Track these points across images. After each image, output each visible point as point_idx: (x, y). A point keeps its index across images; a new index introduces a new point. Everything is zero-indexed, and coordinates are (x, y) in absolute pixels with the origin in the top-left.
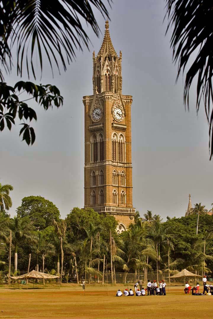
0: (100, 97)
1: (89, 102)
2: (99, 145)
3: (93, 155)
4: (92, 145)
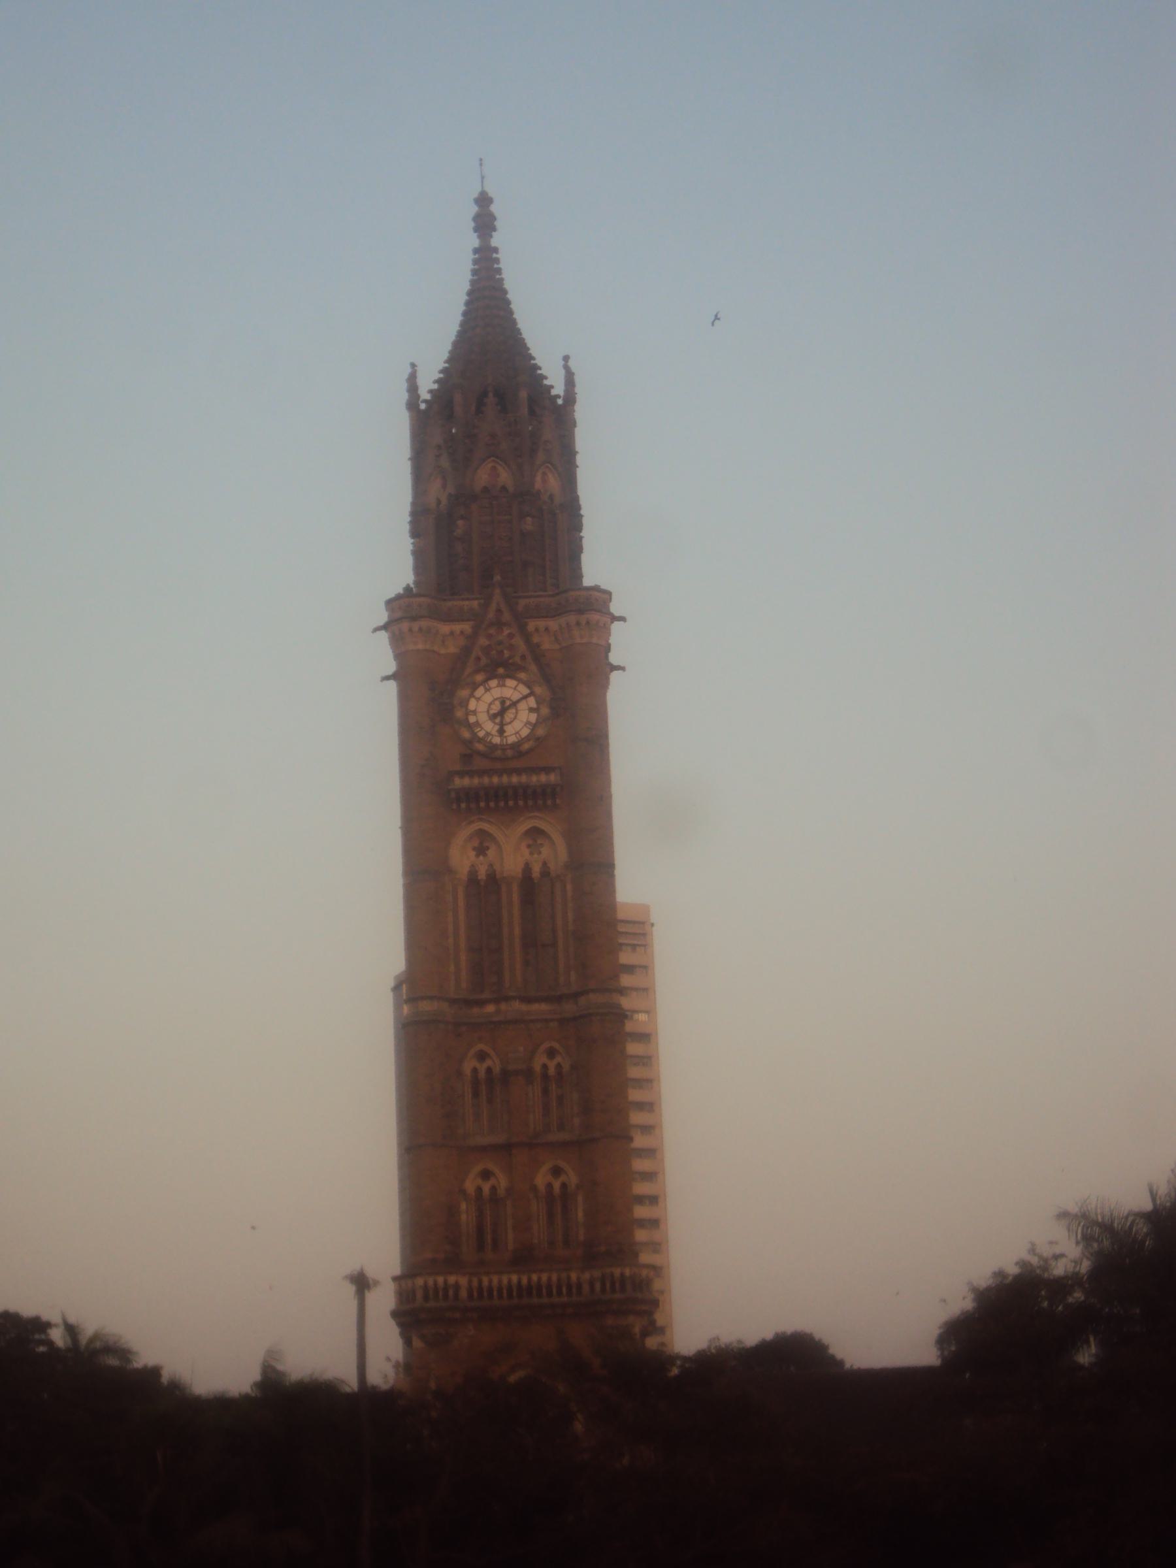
2: (515, 887)
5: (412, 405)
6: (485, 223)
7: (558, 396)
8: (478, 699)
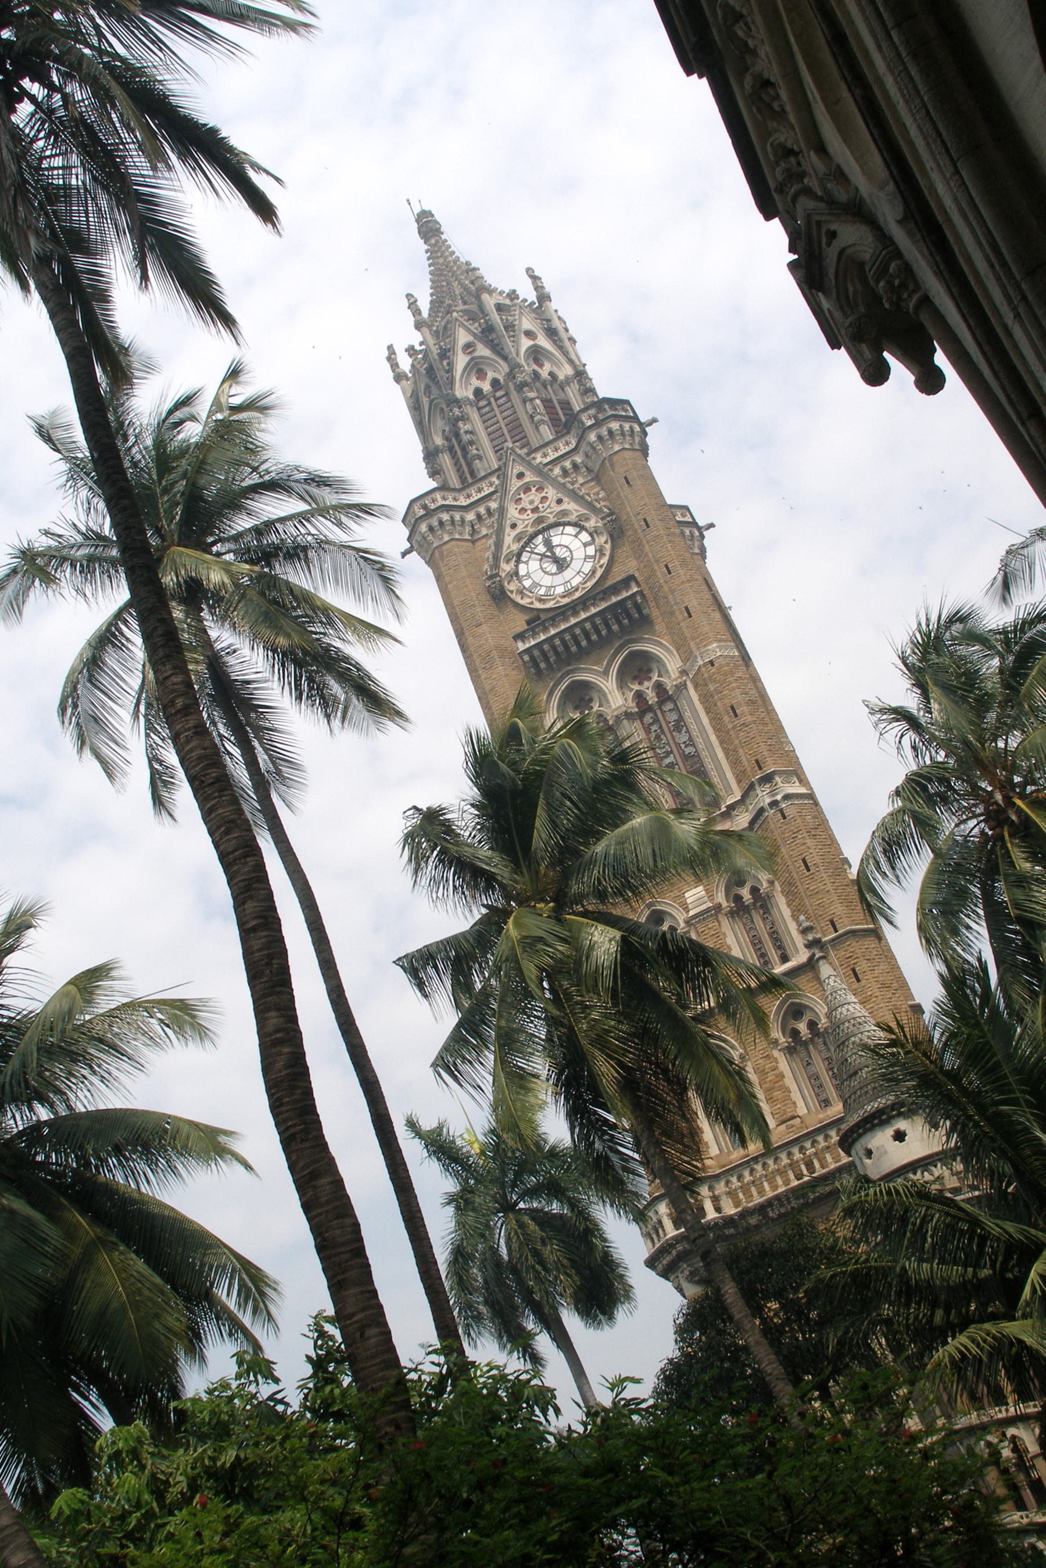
0: (549, 459)
5: (399, 377)
6: (428, 227)
7: (533, 303)
8: (527, 563)
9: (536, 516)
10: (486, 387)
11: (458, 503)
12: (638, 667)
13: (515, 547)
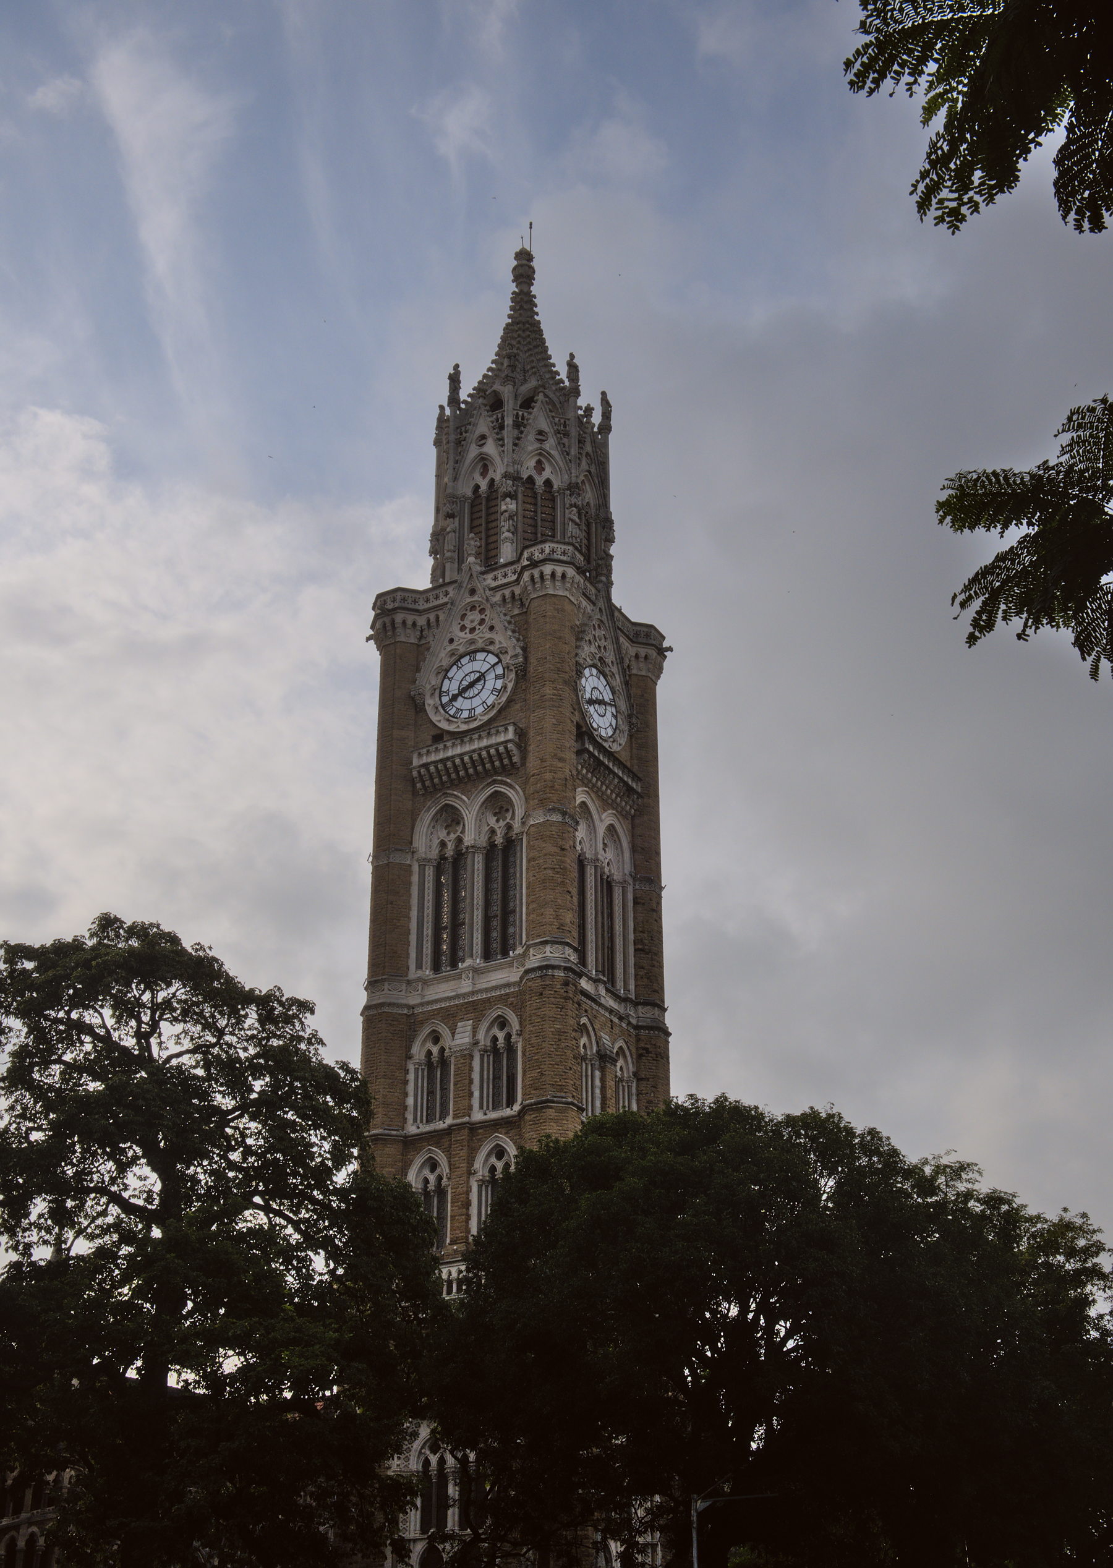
0: (494, 584)
1: (414, 624)
2: (479, 862)
3: (428, 931)
4: (422, 867)
8: (450, 679)
9: (469, 636)
10: (484, 485)
11: (416, 607)
12: (498, 805)
13: (445, 663)
